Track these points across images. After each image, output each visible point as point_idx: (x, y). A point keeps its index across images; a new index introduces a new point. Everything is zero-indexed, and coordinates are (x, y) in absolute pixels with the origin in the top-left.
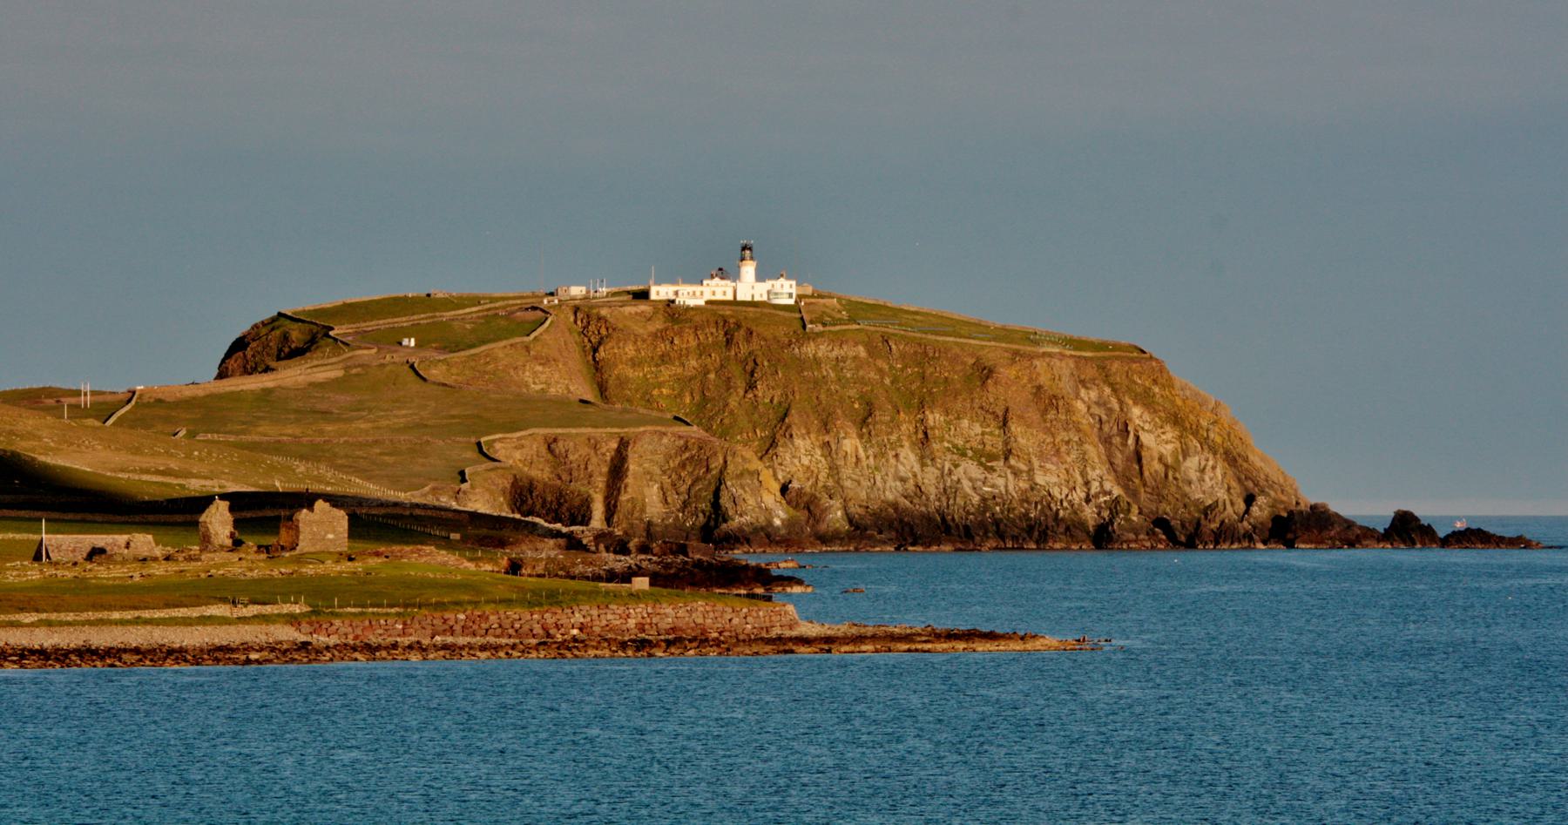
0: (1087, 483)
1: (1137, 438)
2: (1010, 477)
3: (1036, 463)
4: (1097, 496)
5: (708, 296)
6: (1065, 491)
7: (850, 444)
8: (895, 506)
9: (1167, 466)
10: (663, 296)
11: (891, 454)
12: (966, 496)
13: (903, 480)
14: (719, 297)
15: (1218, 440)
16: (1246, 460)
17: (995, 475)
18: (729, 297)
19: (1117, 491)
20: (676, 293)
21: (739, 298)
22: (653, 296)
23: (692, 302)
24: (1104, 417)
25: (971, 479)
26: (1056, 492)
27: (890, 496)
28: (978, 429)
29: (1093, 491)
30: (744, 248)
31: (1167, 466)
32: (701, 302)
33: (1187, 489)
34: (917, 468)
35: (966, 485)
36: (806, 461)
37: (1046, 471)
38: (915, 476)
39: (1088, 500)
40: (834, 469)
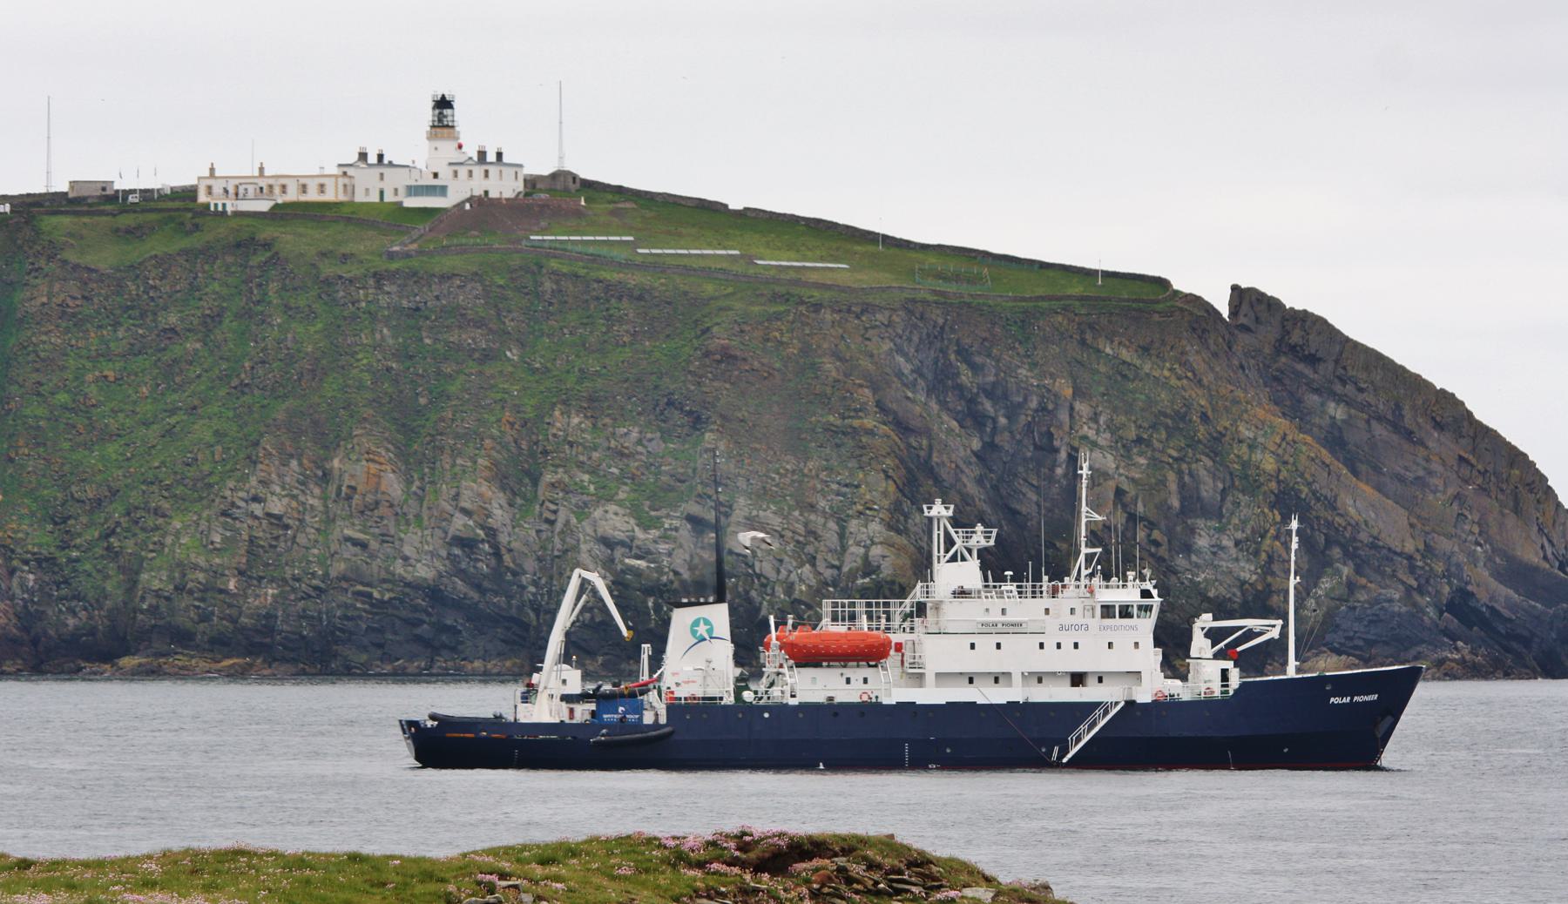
4: (852, 575)
5: (292, 195)
6: (790, 563)
8: (434, 593)
13: (467, 544)
14: (313, 196)
15: (1269, 464)
16: (1332, 505)
17: (654, 533)
21: (360, 197)
22: (202, 198)
23: (245, 206)
24: (1003, 421)
26: (766, 568)
27: (424, 572)
28: (657, 446)
29: (845, 569)
30: (443, 104)
31: (1132, 518)
32: (264, 206)
33: (1180, 561)
34: (500, 515)
36: (276, 506)
38: (492, 533)
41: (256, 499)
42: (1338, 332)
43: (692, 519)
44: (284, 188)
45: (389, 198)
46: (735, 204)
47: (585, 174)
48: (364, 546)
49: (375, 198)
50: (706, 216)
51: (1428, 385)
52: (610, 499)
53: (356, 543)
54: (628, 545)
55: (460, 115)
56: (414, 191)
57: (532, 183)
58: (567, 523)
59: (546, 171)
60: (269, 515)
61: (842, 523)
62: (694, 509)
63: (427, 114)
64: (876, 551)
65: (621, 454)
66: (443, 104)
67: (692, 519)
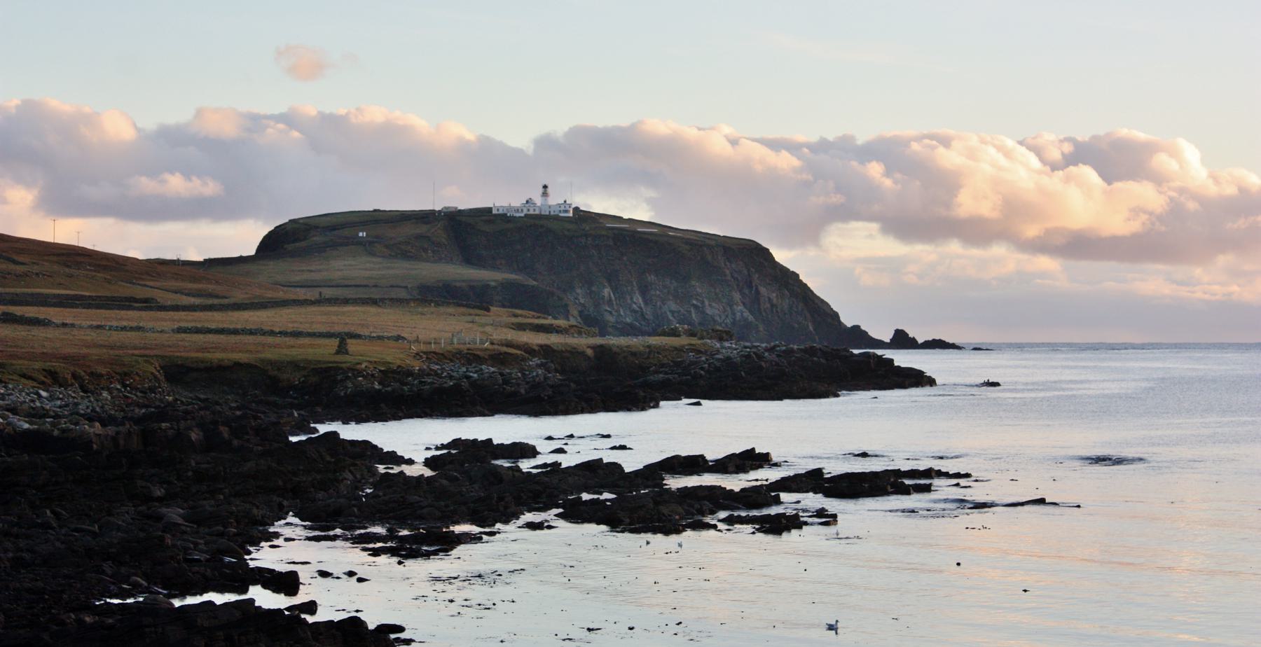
0: (734, 314)
1: (758, 292)
3: (707, 303)
7: (607, 292)
9: (773, 305)
11: (628, 297)
13: (635, 312)
14: (531, 212)
22: (494, 212)
23: (518, 215)
25: (672, 312)
26: (718, 318)
27: (628, 320)
28: (675, 284)
31: (773, 305)
36: (582, 301)
39: (734, 323)
40: (597, 306)
50: (619, 219)
55: (549, 190)
61: (731, 306)
63: (541, 190)
65: (665, 287)
66: (545, 187)
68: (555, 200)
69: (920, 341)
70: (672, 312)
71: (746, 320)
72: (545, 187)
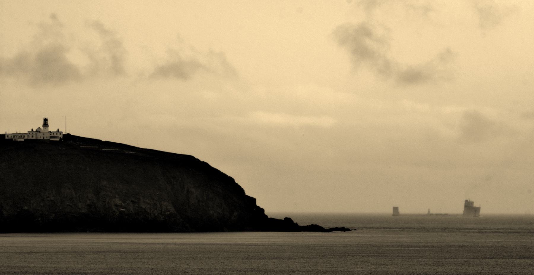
2: (131, 204)
9: (199, 201)
10: (10, 137)
12: (114, 212)
14: (31, 138)
18: (34, 138)
19: (172, 209)
20: (14, 136)
21: (39, 138)
22: (6, 138)
26: (148, 210)
29: (163, 211)
31: (199, 201)
32: (23, 140)
35: (114, 208)
36: (52, 198)
37: (144, 202)
41: (48, 197)
42: (210, 166)
43: (132, 201)
44: (24, 136)
45: (45, 138)
46: (103, 140)
47: (73, 133)
48: (71, 206)
49: (42, 138)
51: (227, 176)
52: (115, 198)
53: (69, 205)
54: (121, 206)
55: (49, 122)
56: (51, 137)
57: (64, 135)
58: (108, 202)
59: (64, 133)
60: (51, 200)
62: (133, 199)
63: (42, 122)
64: (168, 207)
66: (46, 120)
67: (132, 201)
68: (52, 128)
69: (301, 224)
70: (117, 206)
71: (168, 210)
72: (46, 120)
